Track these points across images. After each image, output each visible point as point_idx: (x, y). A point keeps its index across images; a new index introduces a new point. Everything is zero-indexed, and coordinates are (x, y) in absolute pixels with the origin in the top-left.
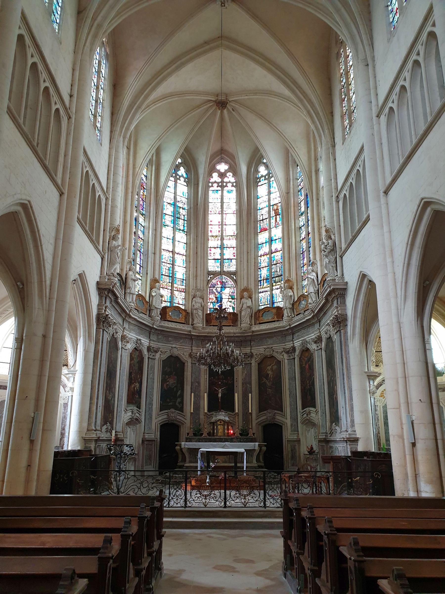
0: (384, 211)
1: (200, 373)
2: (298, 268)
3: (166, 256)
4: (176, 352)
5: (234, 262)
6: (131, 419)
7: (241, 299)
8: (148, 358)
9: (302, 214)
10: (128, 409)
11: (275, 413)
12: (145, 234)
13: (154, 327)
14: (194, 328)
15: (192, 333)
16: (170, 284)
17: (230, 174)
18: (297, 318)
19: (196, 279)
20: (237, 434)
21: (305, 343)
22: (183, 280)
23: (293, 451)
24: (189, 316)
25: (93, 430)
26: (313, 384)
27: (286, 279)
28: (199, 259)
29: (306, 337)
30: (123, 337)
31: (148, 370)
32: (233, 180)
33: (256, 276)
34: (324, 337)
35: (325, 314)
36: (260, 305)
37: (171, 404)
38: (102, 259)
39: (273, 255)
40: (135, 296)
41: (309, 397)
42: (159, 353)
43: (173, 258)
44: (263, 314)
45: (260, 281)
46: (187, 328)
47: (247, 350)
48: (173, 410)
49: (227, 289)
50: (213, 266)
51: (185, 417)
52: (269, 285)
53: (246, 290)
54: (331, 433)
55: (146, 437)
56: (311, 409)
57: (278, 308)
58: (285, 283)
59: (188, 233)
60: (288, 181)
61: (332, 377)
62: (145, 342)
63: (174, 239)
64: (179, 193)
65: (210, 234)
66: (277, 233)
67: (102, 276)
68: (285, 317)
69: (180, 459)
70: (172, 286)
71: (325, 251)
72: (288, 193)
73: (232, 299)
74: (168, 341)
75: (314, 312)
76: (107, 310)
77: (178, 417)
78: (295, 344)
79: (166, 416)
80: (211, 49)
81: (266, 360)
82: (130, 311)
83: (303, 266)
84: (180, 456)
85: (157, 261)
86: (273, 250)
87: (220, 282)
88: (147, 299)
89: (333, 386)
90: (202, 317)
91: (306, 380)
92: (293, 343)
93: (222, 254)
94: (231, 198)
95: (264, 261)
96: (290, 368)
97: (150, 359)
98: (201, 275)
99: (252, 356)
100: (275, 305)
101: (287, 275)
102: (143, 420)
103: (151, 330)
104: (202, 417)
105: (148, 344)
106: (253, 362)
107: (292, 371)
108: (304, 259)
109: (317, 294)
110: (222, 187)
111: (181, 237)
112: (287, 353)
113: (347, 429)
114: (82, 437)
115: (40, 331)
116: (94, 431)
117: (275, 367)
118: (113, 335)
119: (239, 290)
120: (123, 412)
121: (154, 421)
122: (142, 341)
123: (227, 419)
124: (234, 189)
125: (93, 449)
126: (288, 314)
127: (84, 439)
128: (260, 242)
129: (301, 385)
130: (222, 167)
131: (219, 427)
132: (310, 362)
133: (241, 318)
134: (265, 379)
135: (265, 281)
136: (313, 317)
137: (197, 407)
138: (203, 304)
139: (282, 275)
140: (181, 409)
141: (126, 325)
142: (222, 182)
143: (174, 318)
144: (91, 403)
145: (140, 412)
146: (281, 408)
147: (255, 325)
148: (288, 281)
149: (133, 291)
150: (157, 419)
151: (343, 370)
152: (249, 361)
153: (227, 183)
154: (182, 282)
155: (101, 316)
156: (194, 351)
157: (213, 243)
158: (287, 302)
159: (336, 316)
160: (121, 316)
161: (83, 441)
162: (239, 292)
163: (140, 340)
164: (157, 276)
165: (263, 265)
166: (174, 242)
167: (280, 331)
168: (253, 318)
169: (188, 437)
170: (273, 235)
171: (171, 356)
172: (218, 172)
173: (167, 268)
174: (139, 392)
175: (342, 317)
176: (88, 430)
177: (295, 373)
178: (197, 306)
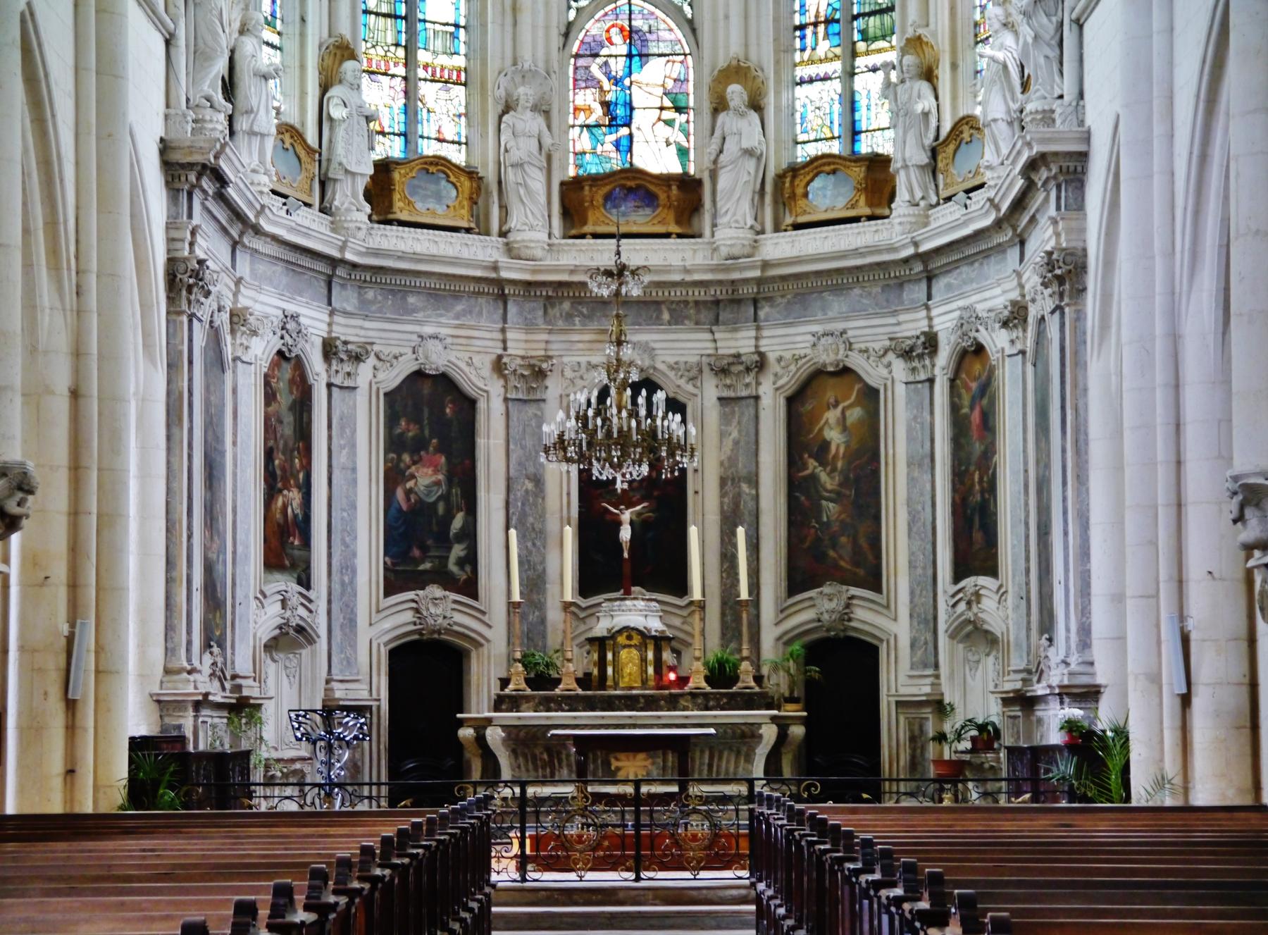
4: (438, 359)
6: (280, 627)
7: (716, 111)
8: (330, 386)
10: (269, 589)
11: (852, 597)
13: (349, 256)
14: (509, 250)
15: (505, 274)
16: (401, 53)
18: (948, 214)
19: (515, 24)
20: (698, 681)
21: (969, 320)
22: (457, 26)
24: (488, 193)
25: (179, 671)
27: (910, 33)
31: (330, 437)
36: (801, 138)
37: (427, 566)
38: (168, 43)
41: (978, 536)
42: (372, 360)
45: (802, 27)
47: (741, 342)
48: (435, 591)
49: (654, 63)
51: (486, 618)
52: (838, 51)
53: (737, 72)
55: (338, 694)
57: (878, 164)
62: (315, 321)
67: (172, 111)
68: (900, 205)
69: (476, 775)
70: (410, 61)
73: (679, 110)
75: (997, 208)
76: (199, 239)
77: (458, 618)
78: (936, 321)
79: (409, 616)
87: (622, 29)
88: (311, 137)
90: (543, 199)
91: (972, 468)
92: (930, 319)
96: (915, 418)
97: (334, 390)
99: (761, 364)
100: (864, 147)
102: (323, 631)
103: (334, 268)
104: (554, 615)
105: (325, 327)
106: (767, 390)
107: (922, 428)
109: (1016, 125)
112: (907, 354)
114: (151, 696)
115: (62, 381)
116: (185, 675)
117: (855, 414)
118: (211, 322)
119: (706, 71)
120: (254, 603)
121: (364, 634)
123: (655, 625)
125: (189, 734)
126: (911, 191)
127: (159, 702)
129: (954, 490)
131: (624, 654)
132: (985, 402)
133: (714, 202)
134: (812, 463)
135: (821, 28)
136: (998, 224)
137: (535, 582)
138: (547, 141)
140: (470, 588)
143: (424, 209)
144: (169, 581)
145: (310, 601)
146: (873, 580)
147: (777, 229)
148: (915, 44)
152: (747, 385)
154: (454, 36)
155: (182, 268)
156: (516, 348)
159: (1050, 254)
161: (155, 706)
162: (707, 80)
163: (295, 317)
164: (344, 29)
167: (878, 264)
168: (768, 199)
169: (507, 691)
171: (418, 375)
175: (1069, 259)
176: (167, 671)
177: (932, 441)
178: (523, 149)
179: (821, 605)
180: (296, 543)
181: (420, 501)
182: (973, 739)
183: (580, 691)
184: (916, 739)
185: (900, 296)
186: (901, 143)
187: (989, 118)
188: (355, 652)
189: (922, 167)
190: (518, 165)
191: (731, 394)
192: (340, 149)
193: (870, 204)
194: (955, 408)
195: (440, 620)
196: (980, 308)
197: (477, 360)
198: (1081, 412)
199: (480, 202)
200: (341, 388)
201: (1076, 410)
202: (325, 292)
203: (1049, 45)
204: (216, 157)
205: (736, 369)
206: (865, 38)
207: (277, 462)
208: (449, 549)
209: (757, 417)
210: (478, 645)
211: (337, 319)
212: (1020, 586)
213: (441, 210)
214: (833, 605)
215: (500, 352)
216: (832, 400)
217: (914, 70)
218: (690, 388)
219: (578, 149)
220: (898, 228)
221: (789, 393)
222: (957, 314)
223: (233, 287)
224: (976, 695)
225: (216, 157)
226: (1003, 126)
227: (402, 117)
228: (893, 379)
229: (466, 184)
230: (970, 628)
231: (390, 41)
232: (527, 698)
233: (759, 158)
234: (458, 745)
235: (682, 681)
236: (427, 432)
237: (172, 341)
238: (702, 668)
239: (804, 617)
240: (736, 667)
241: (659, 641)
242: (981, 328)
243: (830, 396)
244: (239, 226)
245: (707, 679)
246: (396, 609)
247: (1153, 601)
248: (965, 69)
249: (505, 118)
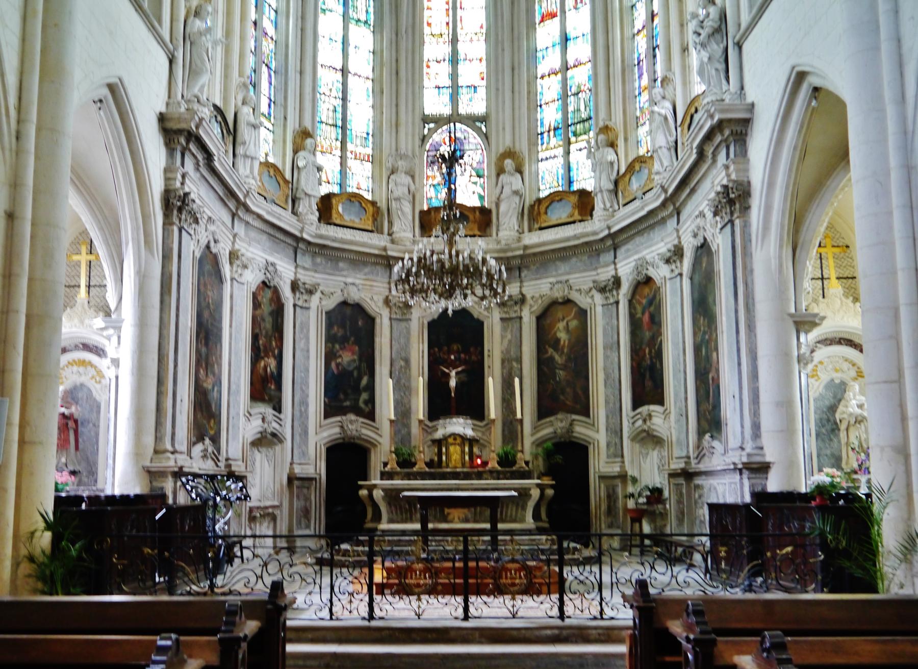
1: (408, 339)
2: (628, 98)
3: (328, 80)
4: (355, 295)
6: (261, 433)
7: (498, 175)
8: (295, 306)
10: (252, 412)
11: (574, 420)
12: (279, 26)
13: (305, 236)
14: (393, 242)
15: (390, 253)
20: (493, 464)
21: (642, 264)
23: (611, 497)
24: (383, 215)
26: (659, 355)
27: (601, 124)
28: (403, 87)
29: (645, 253)
30: (233, 256)
33: (532, 121)
34: (689, 244)
35: (693, 191)
37: (347, 403)
39: (570, 73)
40: (256, 165)
41: (649, 383)
42: (318, 294)
44: (547, 208)
45: (542, 134)
48: (352, 417)
50: (435, 103)
53: (510, 154)
54: (700, 457)
56: (652, 407)
58: (597, 135)
59: (377, 30)
61: (705, 333)
62: (286, 271)
65: (427, 30)
71: (699, 34)
73: (479, 176)
75: (666, 191)
76: (187, 180)
77: (364, 431)
79: (337, 430)
82: (246, 196)
83: (640, 94)
86: (571, 63)
88: (288, 176)
89: (707, 352)
90: (410, 218)
91: (644, 346)
92: (616, 269)
93: (454, 76)
95: (549, 89)
96: (608, 324)
97: (298, 309)
98: (407, 123)
99: (522, 300)
100: (575, 187)
101: (602, 115)
104: (415, 430)
105: (293, 274)
107: (612, 328)
108: (640, 77)
112: (602, 290)
113: (743, 443)
117: (574, 324)
118: (208, 247)
120: (242, 419)
121: (313, 439)
122: (278, 267)
123: (469, 433)
126: (605, 205)
128: (540, 45)
129: (632, 359)
131: (452, 448)
132: (652, 309)
134: (550, 351)
135: (552, 133)
136: (664, 205)
137: (403, 412)
138: (412, 188)
139: (590, 118)
140: (371, 415)
141: (239, 228)
143: (348, 219)
145: (281, 420)
146: (585, 411)
147: (530, 230)
149: (251, 151)
151: (736, 311)
152: (515, 312)
155: (172, 195)
158: (604, 177)
159: (725, 187)
160: (226, 205)
162: (494, 159)
163: (273, 265)
164: (308, 124)
168: (526, 217)
169: (386, 469)
171: (344, 303)
173: (332, 108)
174: (278, 378)
175: (739, 187)
178: (401, 191)
179: (557, 425)
180: (273, 387)
181: (344, 369)
182: (647, 497)
183: (427, 469)
184: (611, 497)
185: (598, 260)
186: (598, 179)
187: (657, 146)
188: (307, 447)
189: (610, 191)
190: (398, 199)
191: (507, 316)
193: (580, 214)
194: (632, 316)
195: (354, 432)
196: (648, 257)
197: (375, 298)
198: (750, 285)
199: (379, 219)
200: (301, 307)
201: (746, 284)
202: (293, 256)
203: (719, 61)
204: (197, 128)
205: (509, 303)
206: (575, 134)
207: (261, 342)
208: (360, 395)
209: (521, 328)
210: (375, 446)
211: (299, 270)
212: (680, 409)
213: (357, 220)
214: (563, 424)
215: (387, 293)
216: (561, 317)
217: (604, 143)
218: (486, 313)
219: (429, 196)
220: (597, 223)
221: (538, 313)
222: (633, 264)
223: (231, 238)
224: (650, 471)
225: (197, 128)
226: (665, 151)
227: (339, 176)
228: (596, 304)
229: (370, 209)
230: (644, 434)
231: (333, 136)
232: (397, 473)
233: (521, 197)
234: (359, 498)
235: (485, 464)
236: (348, 333)
237: (166, 241)
238: (495, 457)
239: (547, 431)
240: (515, 456)
241: (472, 442)
242: (650, 268)
243: (560, 315)
244: (229, 196)
245: (499, 463)
246: (331, 426)
247: (896, 386)
248: (632, 141)
249: (392, 177)
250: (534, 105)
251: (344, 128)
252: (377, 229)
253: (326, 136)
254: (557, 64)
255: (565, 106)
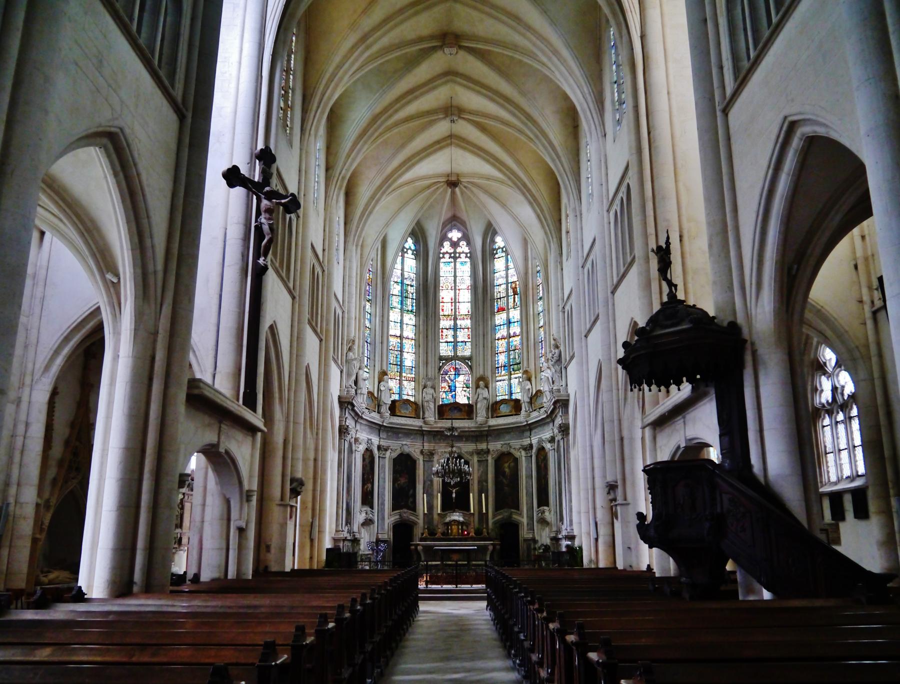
0: (584, 353)
3: (393, 341)
4: (407, 450)
5: (469, 344)
9: (541, 298)
14: (425, 423)
17: (463, 243)
20: (472, 534)
21: (540, 441)
28: (430, 344)
32: (467, 250)
33: (493, 361)
43: (401, 343)
46: (416, 423)
47: (483, 446)
50: (445, 350)
53: (482, 378)
56: (545, 508)
57: (517, 401)
59: (417, 314)
60: (526, 259)
62: (375, 440)
63: (402, 322)
64: (406, 269)
65: (441, 313)
66: (515, 314)
68: (523, 412)
70: (401, 376)
72: (526, 273)
74: (398, 438)
80: (441, 148)
81: (504, 457)
84: (415, 557)
85: (385, 351)
88: (376, 395)
93: (455, 336)
94: (464, 270)
95: (501, 345)
100: (514, 397)
104: (436, 517)
106: (490, 458)
110: (455, 258)
111: (410, 319)
115: (312, 456)
117: (512, 464)
121: (387, 521)
123: (461, 519)
124: (468, 260)
128: (497, 322)
130: (455, 235)
136: (547, 417)
137: (431, 507)
141: (358, 427)
142: (455, 253)
143: (403, 412)
148: (526, 372)
150: (390, 519)
153: (460, 253)
157: (444, 323)
164: (385, 368)
165: (501, 350)
166: (403, 324)
170: (511, 317)
171: (401, 455)
172: (450, 240)
179: (503, 514)
190: (427, 401)
192: (383, 397)
224: (544, 537)
235: (468, 534)
239: (499, 517)
241: (462, 523)
244: (357, 417)
248: (538, 378)
250: (495, 353)
251: (401, 366)
252: (417, 417)
253: (393, 371)
254: (505, 334)
255: (509, 355)
